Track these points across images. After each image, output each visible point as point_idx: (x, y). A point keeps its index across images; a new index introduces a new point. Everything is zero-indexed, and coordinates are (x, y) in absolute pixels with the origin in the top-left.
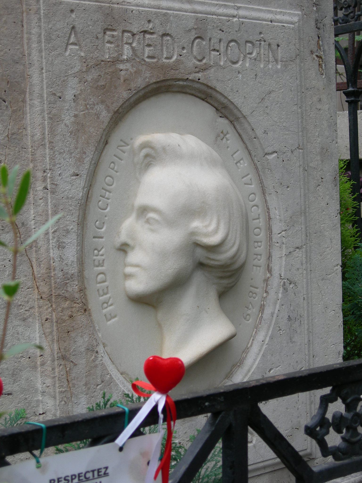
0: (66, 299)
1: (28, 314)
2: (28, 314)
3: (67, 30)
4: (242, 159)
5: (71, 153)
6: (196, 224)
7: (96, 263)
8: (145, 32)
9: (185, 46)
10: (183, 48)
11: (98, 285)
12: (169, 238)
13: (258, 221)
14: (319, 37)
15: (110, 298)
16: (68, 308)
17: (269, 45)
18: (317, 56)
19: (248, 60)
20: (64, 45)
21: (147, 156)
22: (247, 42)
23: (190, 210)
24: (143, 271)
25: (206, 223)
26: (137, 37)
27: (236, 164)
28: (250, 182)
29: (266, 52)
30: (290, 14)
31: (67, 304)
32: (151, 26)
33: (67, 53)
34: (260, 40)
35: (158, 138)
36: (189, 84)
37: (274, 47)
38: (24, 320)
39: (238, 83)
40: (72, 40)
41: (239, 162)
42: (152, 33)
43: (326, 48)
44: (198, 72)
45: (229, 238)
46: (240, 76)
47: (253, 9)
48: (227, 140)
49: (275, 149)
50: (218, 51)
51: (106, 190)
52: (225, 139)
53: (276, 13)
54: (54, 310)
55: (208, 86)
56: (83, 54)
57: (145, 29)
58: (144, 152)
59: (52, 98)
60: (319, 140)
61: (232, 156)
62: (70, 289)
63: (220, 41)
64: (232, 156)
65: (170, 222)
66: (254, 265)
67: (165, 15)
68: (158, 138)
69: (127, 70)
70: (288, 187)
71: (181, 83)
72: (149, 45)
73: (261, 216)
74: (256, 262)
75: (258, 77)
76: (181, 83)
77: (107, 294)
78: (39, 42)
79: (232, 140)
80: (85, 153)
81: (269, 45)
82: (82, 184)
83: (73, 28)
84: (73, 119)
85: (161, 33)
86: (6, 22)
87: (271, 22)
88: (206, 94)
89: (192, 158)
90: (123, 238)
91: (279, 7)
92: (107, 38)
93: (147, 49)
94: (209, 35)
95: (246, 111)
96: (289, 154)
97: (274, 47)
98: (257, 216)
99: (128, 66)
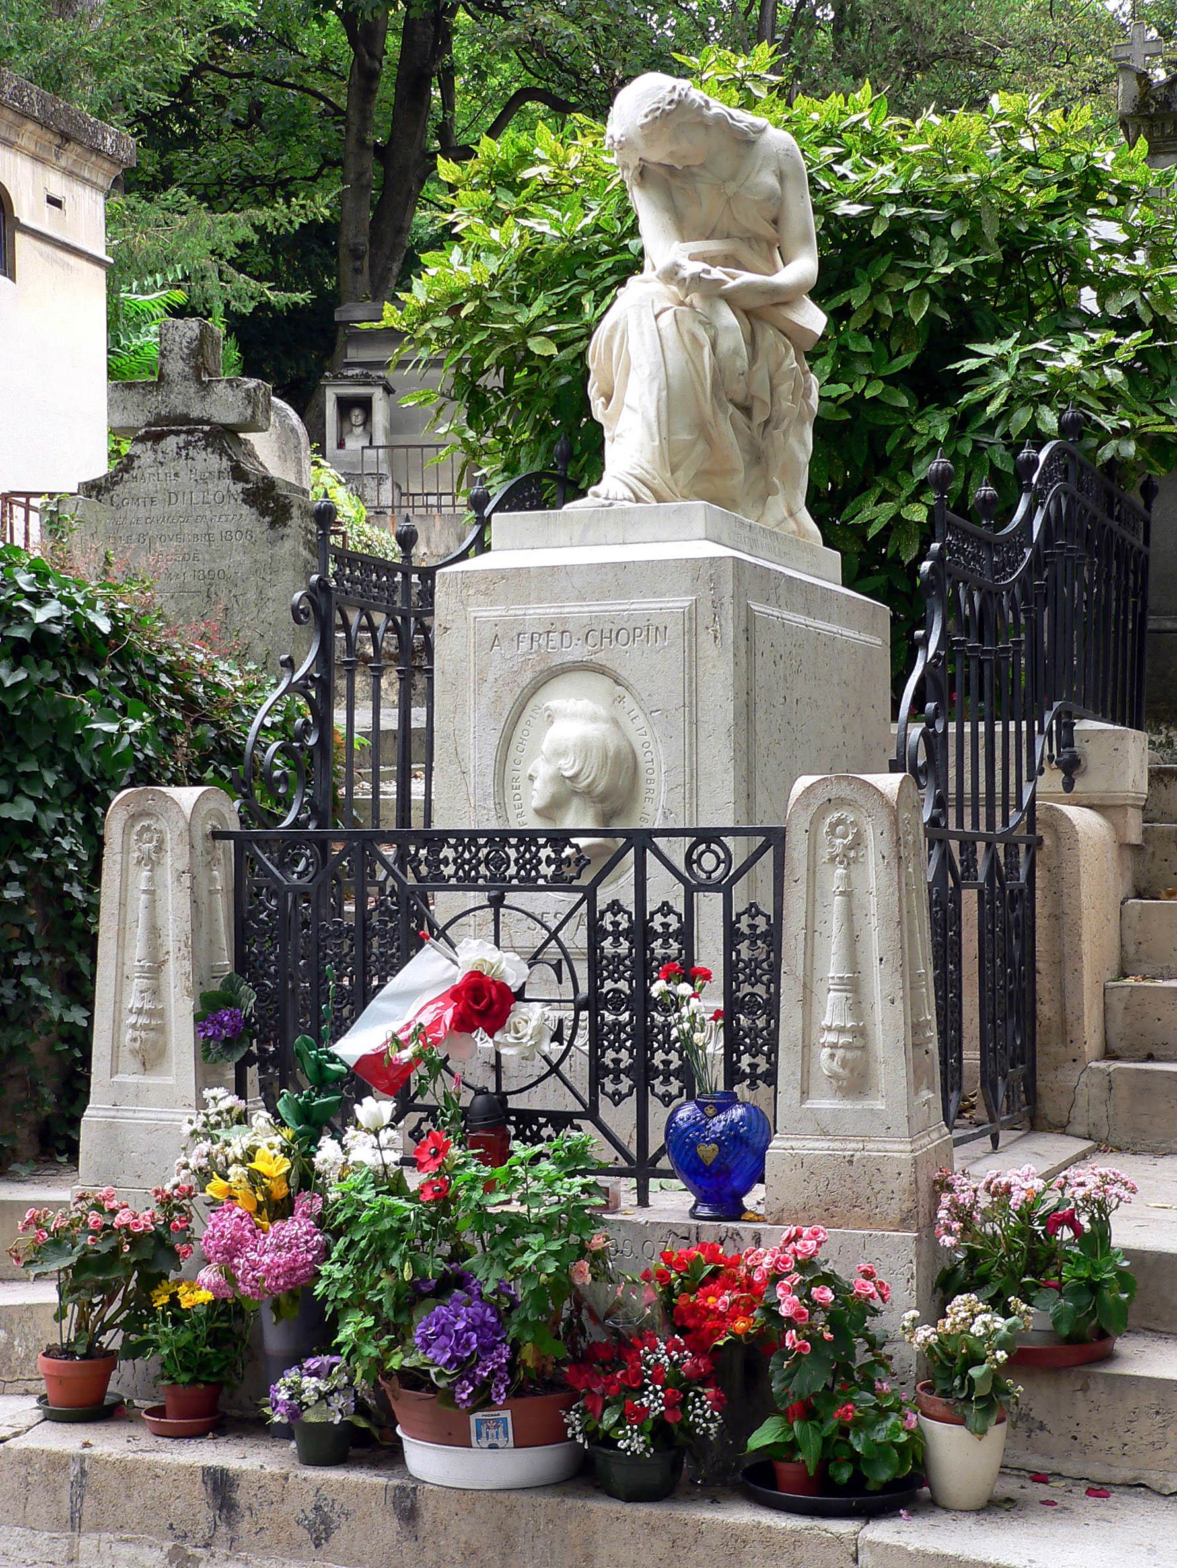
6: (562, 762)
23: (559, 753)
24: (539, 794)
35: (554, 704)
37: (662, 629)
39: (628, 659)
68: (554, 704)
88: (602, 670)
89: (574, 715)
90: (529, 771)
97: (662, 629)
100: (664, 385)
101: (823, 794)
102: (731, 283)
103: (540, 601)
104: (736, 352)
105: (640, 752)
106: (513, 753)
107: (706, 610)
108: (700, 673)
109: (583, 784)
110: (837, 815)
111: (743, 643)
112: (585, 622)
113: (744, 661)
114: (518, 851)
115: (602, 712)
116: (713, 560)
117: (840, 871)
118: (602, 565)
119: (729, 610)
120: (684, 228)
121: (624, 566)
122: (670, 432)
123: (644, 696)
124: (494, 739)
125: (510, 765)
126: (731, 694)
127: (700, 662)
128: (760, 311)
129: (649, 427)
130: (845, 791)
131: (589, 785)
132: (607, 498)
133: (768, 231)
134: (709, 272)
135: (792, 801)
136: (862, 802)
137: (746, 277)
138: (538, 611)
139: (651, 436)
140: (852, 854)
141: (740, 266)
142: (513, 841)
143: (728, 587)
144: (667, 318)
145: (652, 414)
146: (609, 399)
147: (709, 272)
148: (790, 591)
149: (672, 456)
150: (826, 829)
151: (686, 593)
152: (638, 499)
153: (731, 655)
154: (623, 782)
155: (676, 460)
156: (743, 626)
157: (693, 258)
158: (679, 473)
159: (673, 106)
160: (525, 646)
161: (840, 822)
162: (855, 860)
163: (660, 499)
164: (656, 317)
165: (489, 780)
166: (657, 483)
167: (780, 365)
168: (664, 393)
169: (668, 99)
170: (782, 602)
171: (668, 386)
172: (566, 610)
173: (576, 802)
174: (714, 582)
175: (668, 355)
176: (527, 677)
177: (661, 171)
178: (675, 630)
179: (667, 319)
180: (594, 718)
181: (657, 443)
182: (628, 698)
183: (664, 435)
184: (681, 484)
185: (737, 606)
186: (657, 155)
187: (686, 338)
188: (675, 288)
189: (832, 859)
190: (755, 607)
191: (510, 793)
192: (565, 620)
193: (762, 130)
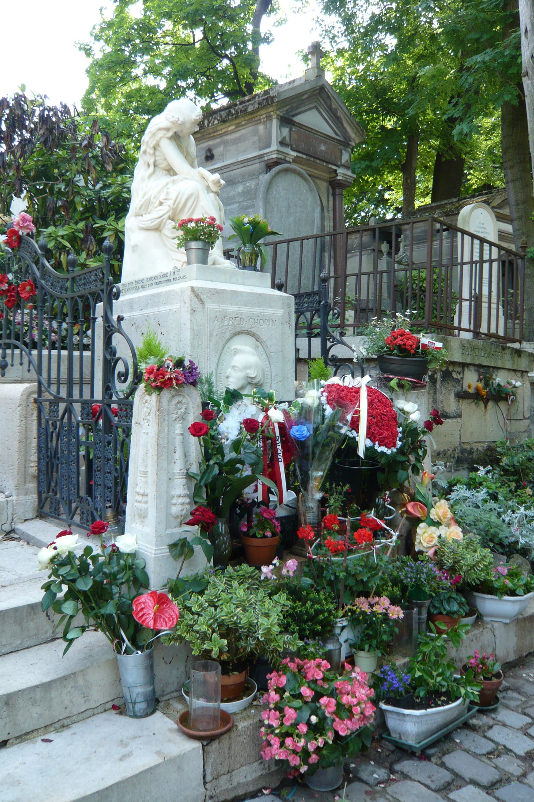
6: (248, 371)
12: (241, 375)
23: (247, 367)
35: (238, 347)
39: (263, 331)
65: (241, 370)
88: (253, 335)
109: (255, 381)
121: (260, 295)
138: (232, 309)
160: (226, 322)
176: (228, 335)
182: (260, 347)
192: (242, 314)
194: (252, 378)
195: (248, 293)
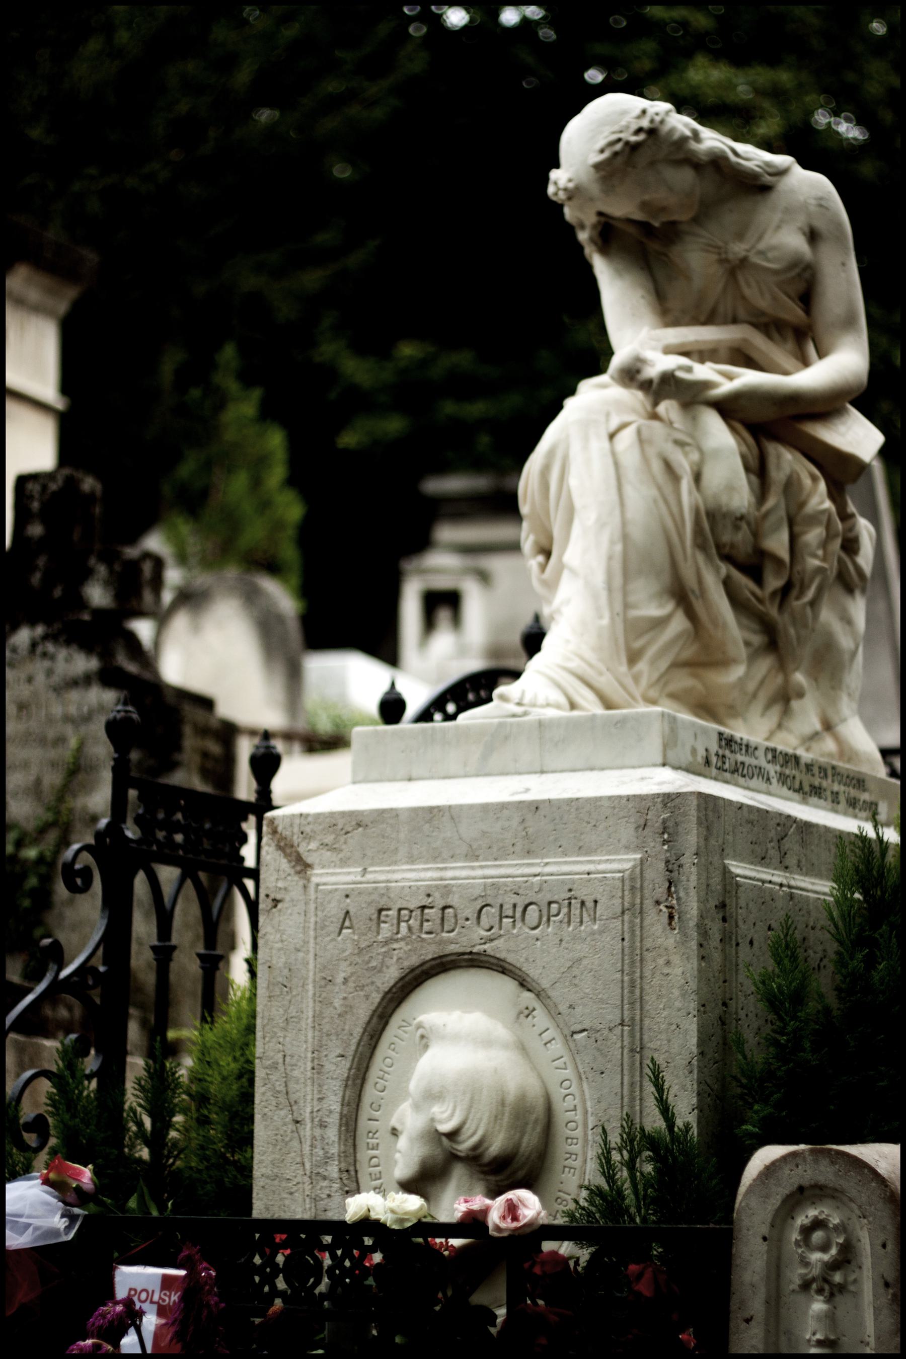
0: (325, 1178)
1: (295, 1188)
2: (295, 1188)
3: (342, 916)
4: (554, 1039)
5: (338, 1035)
7: (370, 1146)
8: (423, 908)
9: (469, 916)
10: (467, 919)
11: (371, 1169)
13: (573, 1113)
14: (670, 883)
15: (382, 1184)
16: (326, 1187)
17: (583, 903)
18: (667, 907)
19: (551, 923)
20: (337, 930)
21: (422, 1037)
22: (550, 903)
23: (432, 1095)
24: (405, 1158)
25: (443, 1109)
26: (414, 914)
27: (546, 1044)
28: (563, 1066)
29: (578, 912)
30: (620, 861)
31: (326, 1183)
32: (430, 900)
33: (340, 938)
34: (570, 898)
36: (475, 957)
38: (291, 1193)
40: (347, 924)
41: (550, 1042)
42: (432, 908)
43: (682, 894)
44: (485, 943)
45: (467, 1126)
46: (539, 943)
47: (566, 863)
48: (534, 1017)
49: (585, 1027)
50: (512, 917)
51: (385, 1072)
52: (530, 1017)
53: (600, 862)
54: (313, 1188)
55: (498, 959)
56: (356, 937)
57: (423, 904)
58: (420, 1031)
59: (323, 983)
60: (665, 1013)
61: (540, 1035)
62: (329, 1168)
63: (515, 906)
64: (540, 1035)
66: (565, 1167)
67: (446, 886)
69: (400, 949)
70: (602, 1073)
71: (466, 957)
72: (428, 921)
73: (578, 1108)
74: (570, 1162)
75: (563, 943)
76: (466, 957)
77: (380, 1178)
78: (315, 929)
79: (541, 1017)
80: (352, 1034)
81: (583, 903)
82: (348, 1066)
83: (347, 912)
84: (342, 1002)
85: (441, 906)
86: (291, 914)
87: (589, 874)
88: (501, 967)
89: (456, 1038)
90: (394, 1122)
91: (609, 853)
92: (382, 918)
93: (425, 924)
94: (500, 901)
95: (545, 983)
96: (606, 1032)
98: (572, 1107)
99: (402, 944)
100: (617, 534)
101: (791, 1179)
102: (726, 387)
103: (412, 860)
104: (730, 488)
105: (557, 1094)
106: (370, 1093)
107: (656, 875)
108: (647, 973)
109: (465, 1145)
110: (812, 1213)
111: (715, 928)
112: (477, 892)
113: (717, 957)
114: (333, 1256)
115: (501, 1031)
116: (668, 800)
117: (818, 1306)
118: (503, 806)
119: (691, 877)
120: (668, 312)
121: (536, 806)
122: (626, 606)
123: (563, 1008)
124: (338, 1069)
125: (366, 1111)
126: (693, 1006)
127: (648, 956)
128: (771, 423)
129: (595, 597)
130: (825, 1173)
131: (475, 1148)
132: (519, 704)
133: (794, 312)
134: (689, 370)
135: (742, 1189)
136: (853, 1193)
137: (748, 378)
138: (409, 877)
139: (598, 609)
140: (838, 1278)
141: (750, 362)
142: (328, 1239)
143: (691, 838)
144: (627, 438)
145: (599, 578)
146: (548, 554)
147: (689, 370)
148: (803, 843)
149: (633, 638)
150: (795, 1236)
151: (627, 848)
152: (573, 706)
153: (694, 944)
154: (530, 1141)
155: (638, 644)
156: (713, 903)
157: (668, 350)
158: (642, 666)
159: (641, 137)
160: (386, 929)
161: (818, 1224)
162: (842, 1288)
163: (608, 705)
164: (612, 436)
165: (332, 1134)
166: (605, 681)
167: (802, 505)
168: (619, 548)
169: (634, 127)
170: (791, 860)
171: (625, 537)
172: (449, 874)
173: (459, 1172)
174: (669, 832)
175: (630, 492)
176: (391, 975)
177: (631, 230)
178: (609, 906)
179: (627, 438)
180: (487, 1043)
181: (605, 621)
183: (618, 607)
184: (644, 682)
185: (705, 869)
186: (622, 208)
187: (657, 467)
188: (640, 394)
189: (806, 1286)
190: (738, 868)
191: (363, 1154)
192: (447, 890)
193: (782, 172)
194: (453, 1135)
195: (485, 808)
